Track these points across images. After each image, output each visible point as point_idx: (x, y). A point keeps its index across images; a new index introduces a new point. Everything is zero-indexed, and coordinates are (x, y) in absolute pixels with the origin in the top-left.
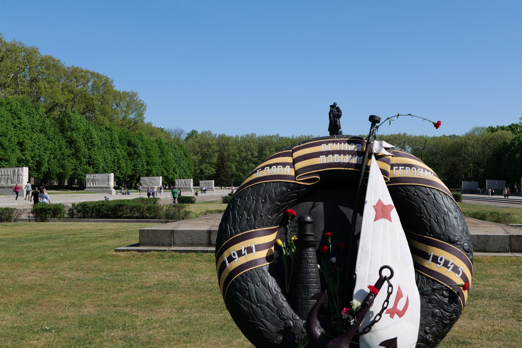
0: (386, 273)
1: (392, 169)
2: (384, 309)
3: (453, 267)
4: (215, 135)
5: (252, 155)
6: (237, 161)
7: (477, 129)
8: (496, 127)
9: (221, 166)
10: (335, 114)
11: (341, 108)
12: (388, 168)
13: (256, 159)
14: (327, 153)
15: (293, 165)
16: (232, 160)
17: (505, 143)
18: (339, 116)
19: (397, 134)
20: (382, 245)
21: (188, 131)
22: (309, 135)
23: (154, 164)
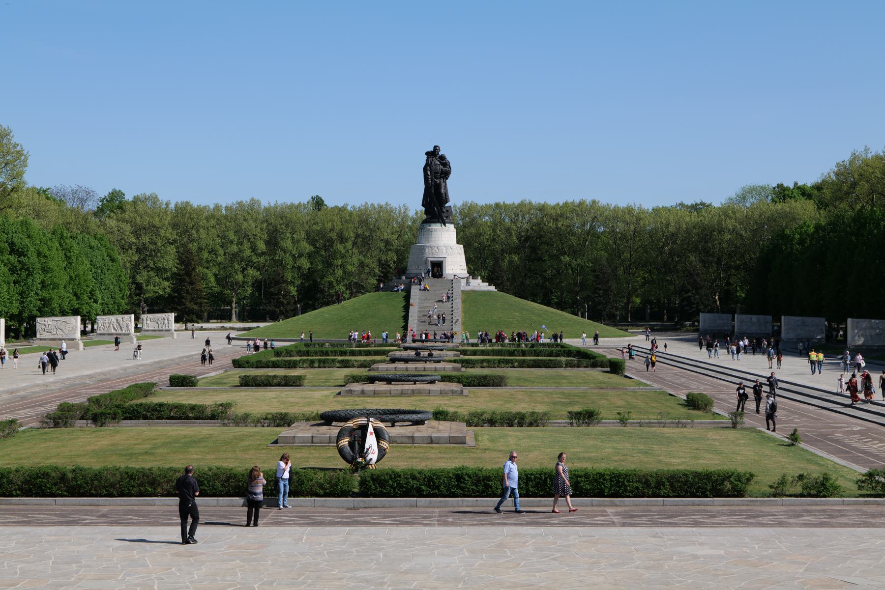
3: (385, 445)
4: (167, 204)
5: (254, 249)
6: (219, 264)
7: (751, 190)
8: (792, 186)
9: (185, 274)
10: (436, 169)
11: (448, 158)
13: (262, 259)
16: (208, 262)
17: (781, 237)
18: (446, 174)
19: (577, 201)
20: (371, 440)
21: (103, 192)
22: (383, 203)
23: (56, 286)
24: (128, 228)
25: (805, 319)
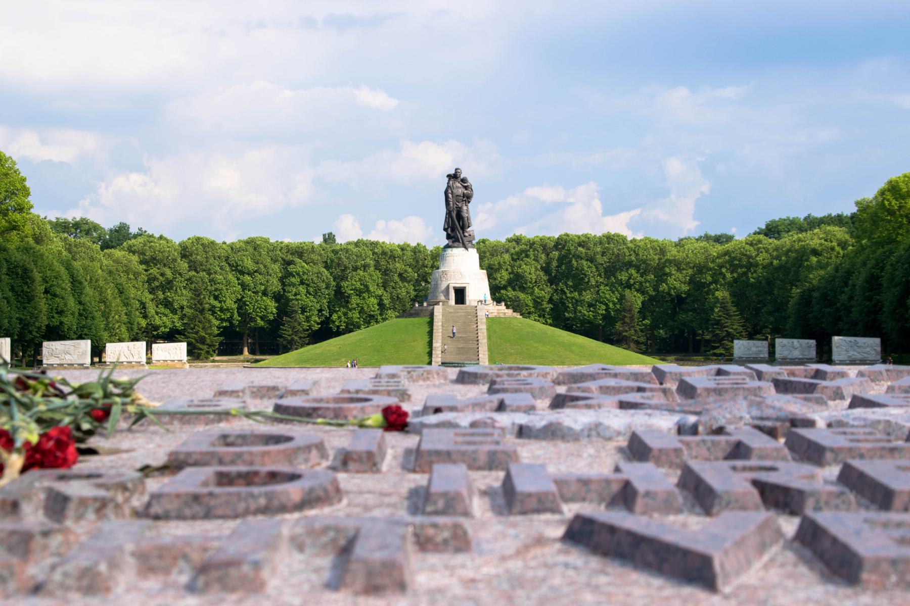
11: (471, 181)
18: (467, 198)
24: (135, 258)
25: (859, 339)
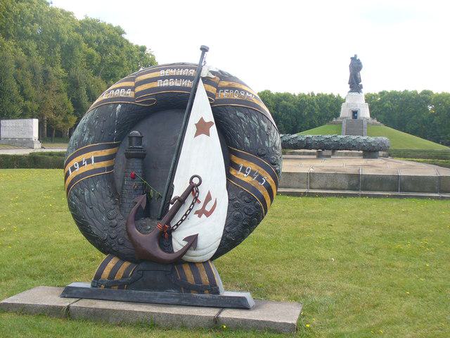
0: (196, 181)
1: (218, 91)
2: (190, 210)
10: (356, 66)
11: (361, 61)
12: (213, 90)
14: (163, 78)
15: (133, 89)
